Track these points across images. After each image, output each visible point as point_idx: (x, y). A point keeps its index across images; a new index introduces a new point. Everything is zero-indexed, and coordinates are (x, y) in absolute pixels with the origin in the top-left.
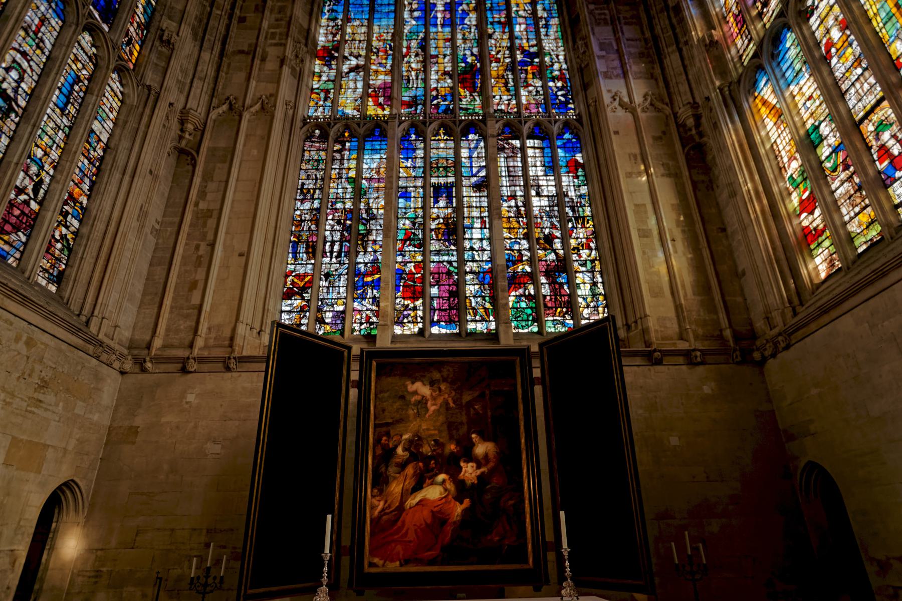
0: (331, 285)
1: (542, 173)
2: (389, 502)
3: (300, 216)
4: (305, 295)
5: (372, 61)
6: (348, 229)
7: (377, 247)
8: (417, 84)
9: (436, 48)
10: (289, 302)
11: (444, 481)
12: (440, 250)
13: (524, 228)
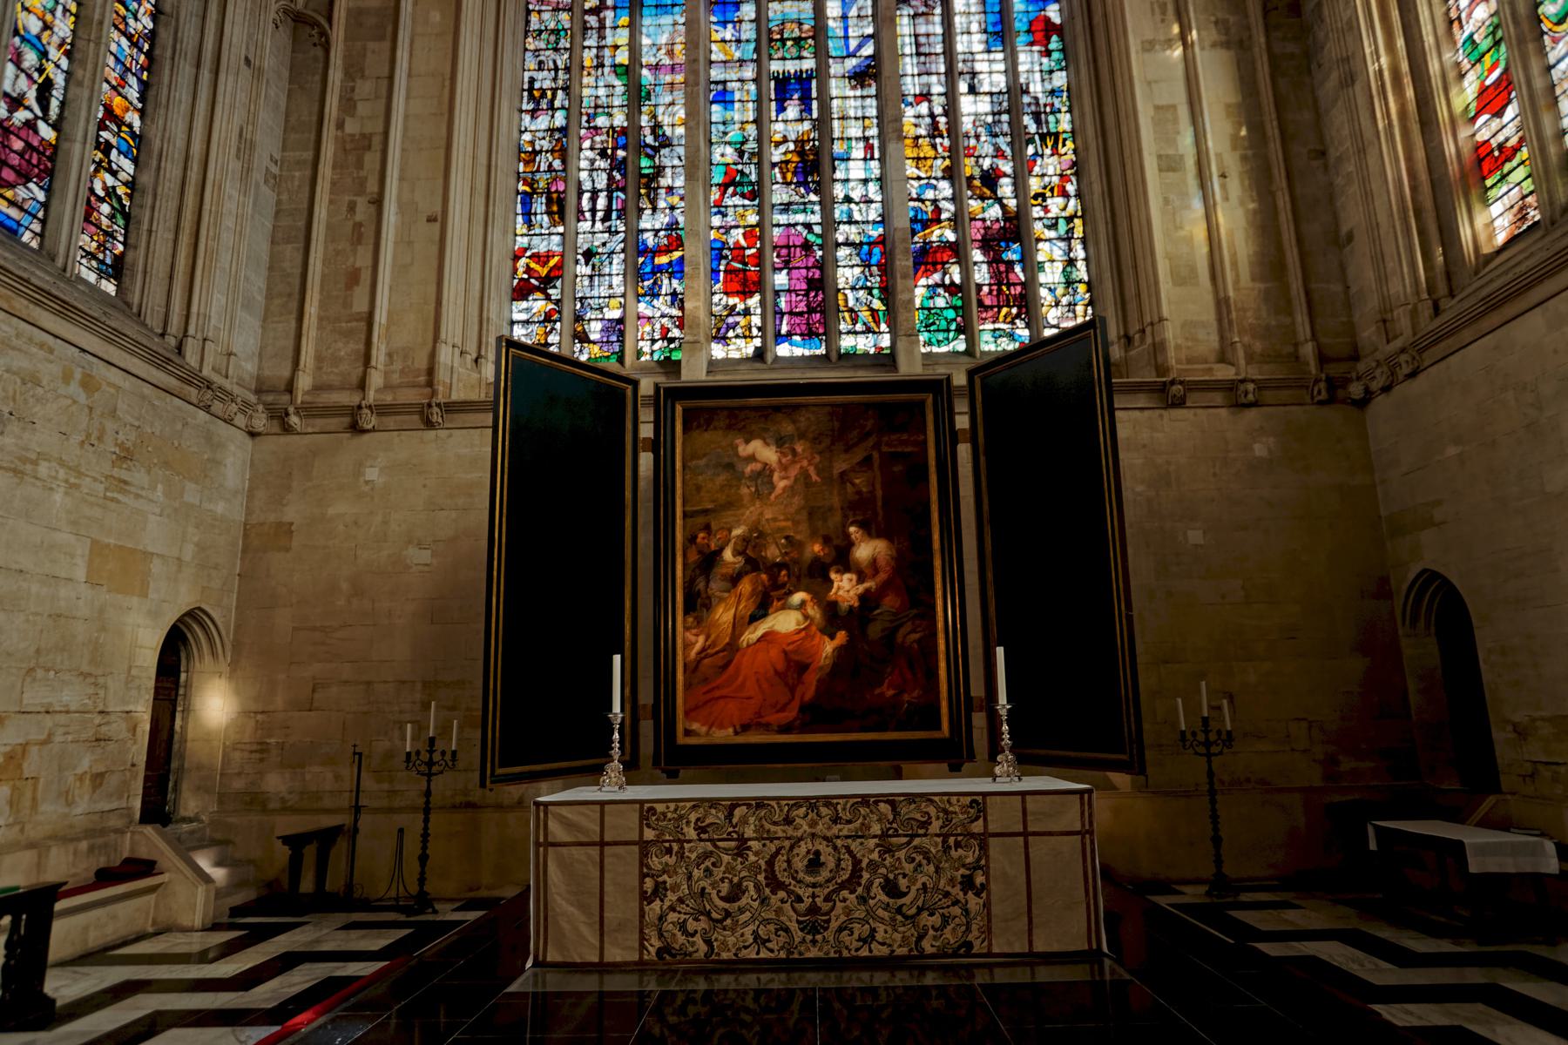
1: (981, 47)
2: (713, 637)
3: (532, 143)
4: (550, 291)
6: (620, 165)
7: (675, 200)
10: (524, 304)
11: (803, 604)
12: (790, 204)
13: (944, 158)
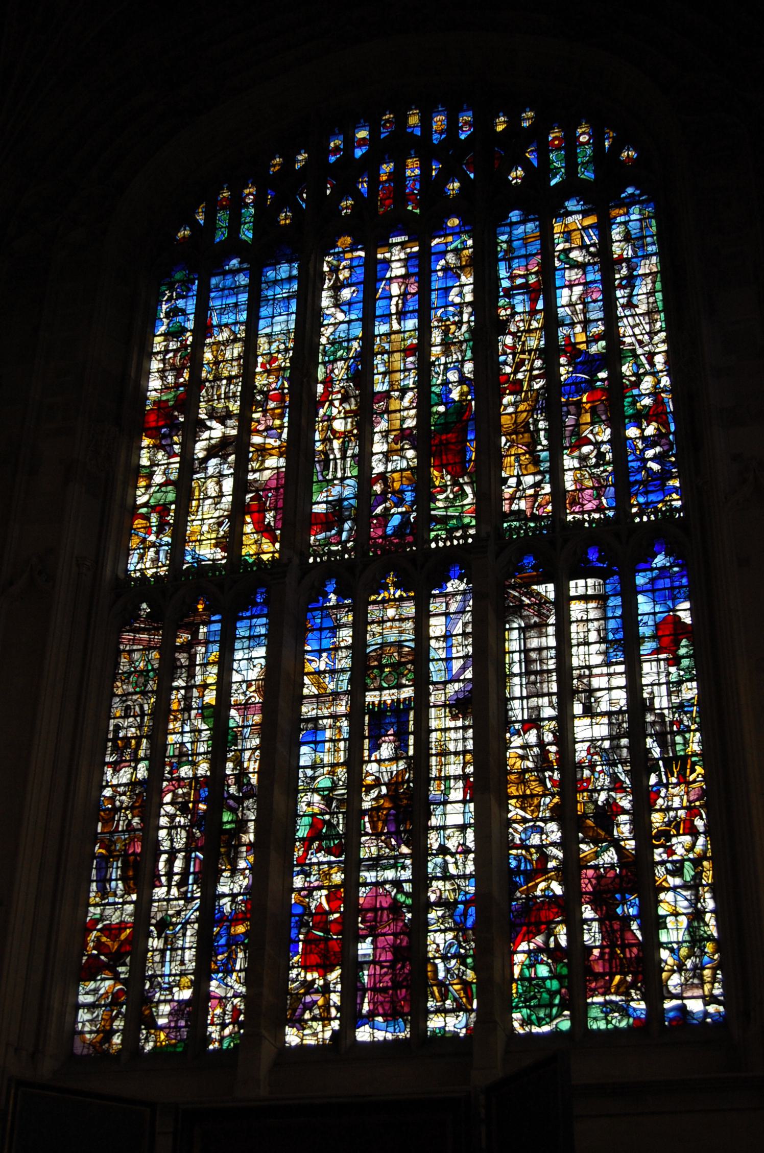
0: (170, 945)
1: (597, 660)
3: (112, 799)
5: (254, 425)
8: (344, 469)
9: (384, 374)
10: (92, 985)
12: (379, 857)
